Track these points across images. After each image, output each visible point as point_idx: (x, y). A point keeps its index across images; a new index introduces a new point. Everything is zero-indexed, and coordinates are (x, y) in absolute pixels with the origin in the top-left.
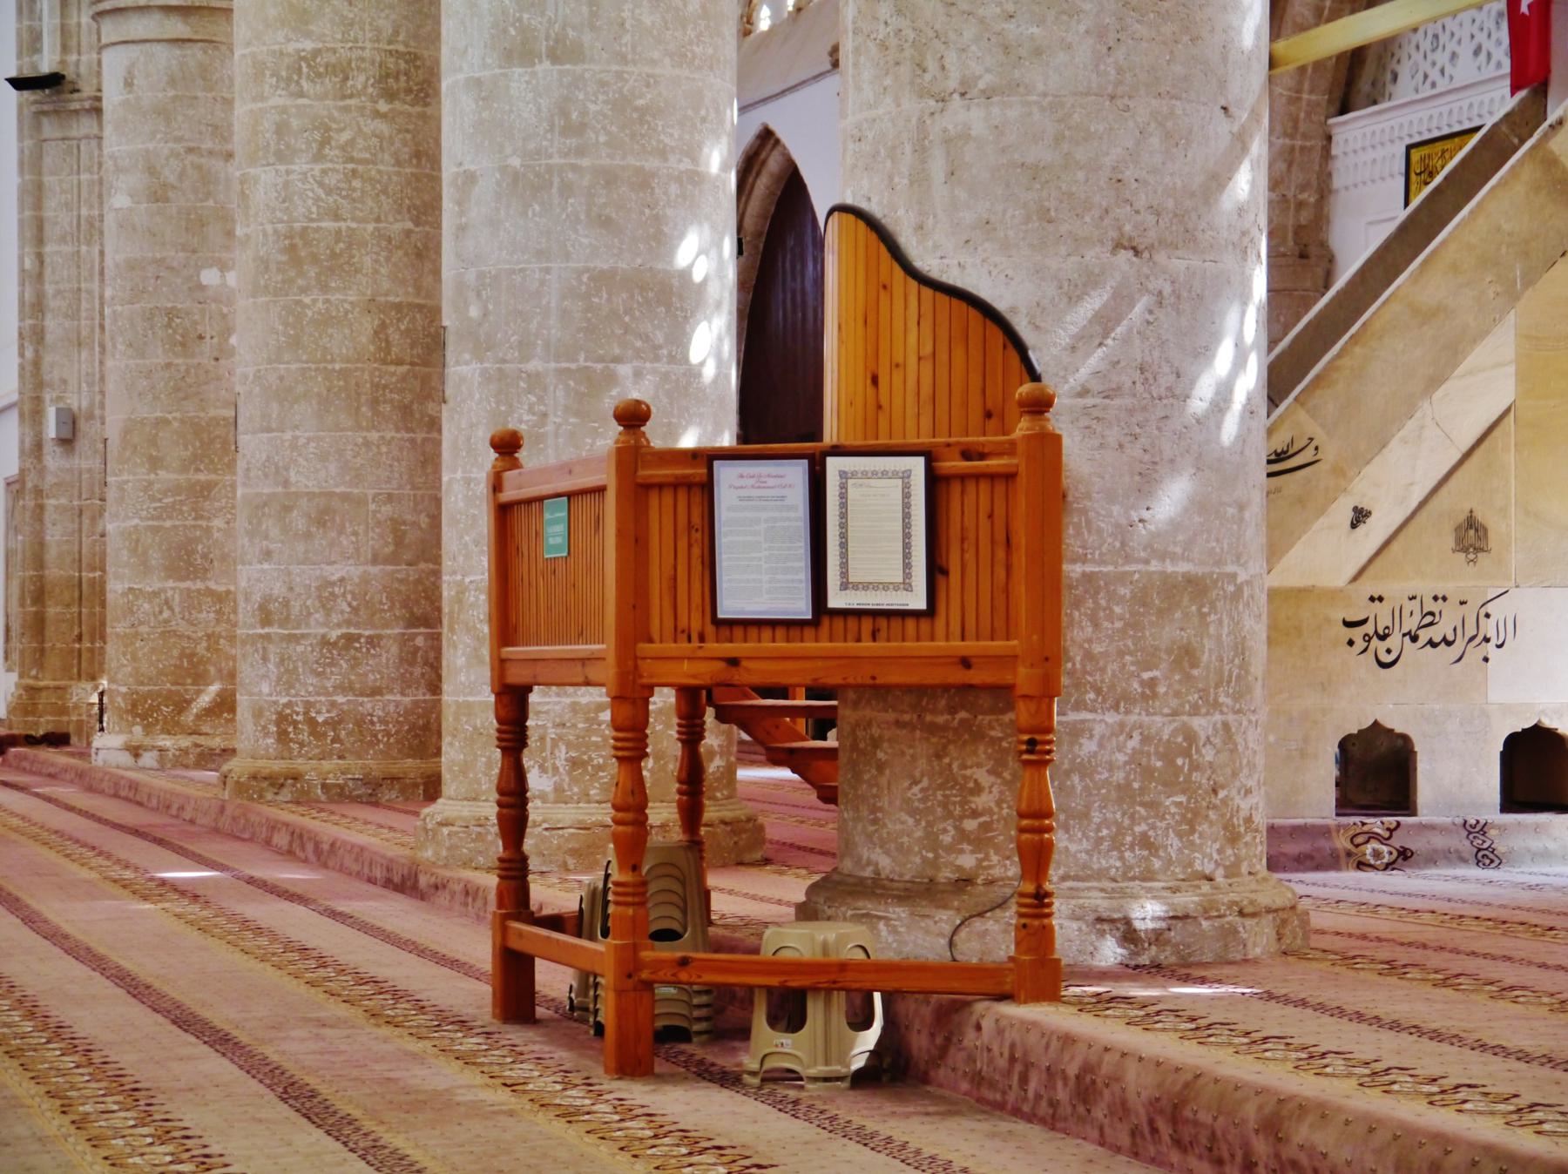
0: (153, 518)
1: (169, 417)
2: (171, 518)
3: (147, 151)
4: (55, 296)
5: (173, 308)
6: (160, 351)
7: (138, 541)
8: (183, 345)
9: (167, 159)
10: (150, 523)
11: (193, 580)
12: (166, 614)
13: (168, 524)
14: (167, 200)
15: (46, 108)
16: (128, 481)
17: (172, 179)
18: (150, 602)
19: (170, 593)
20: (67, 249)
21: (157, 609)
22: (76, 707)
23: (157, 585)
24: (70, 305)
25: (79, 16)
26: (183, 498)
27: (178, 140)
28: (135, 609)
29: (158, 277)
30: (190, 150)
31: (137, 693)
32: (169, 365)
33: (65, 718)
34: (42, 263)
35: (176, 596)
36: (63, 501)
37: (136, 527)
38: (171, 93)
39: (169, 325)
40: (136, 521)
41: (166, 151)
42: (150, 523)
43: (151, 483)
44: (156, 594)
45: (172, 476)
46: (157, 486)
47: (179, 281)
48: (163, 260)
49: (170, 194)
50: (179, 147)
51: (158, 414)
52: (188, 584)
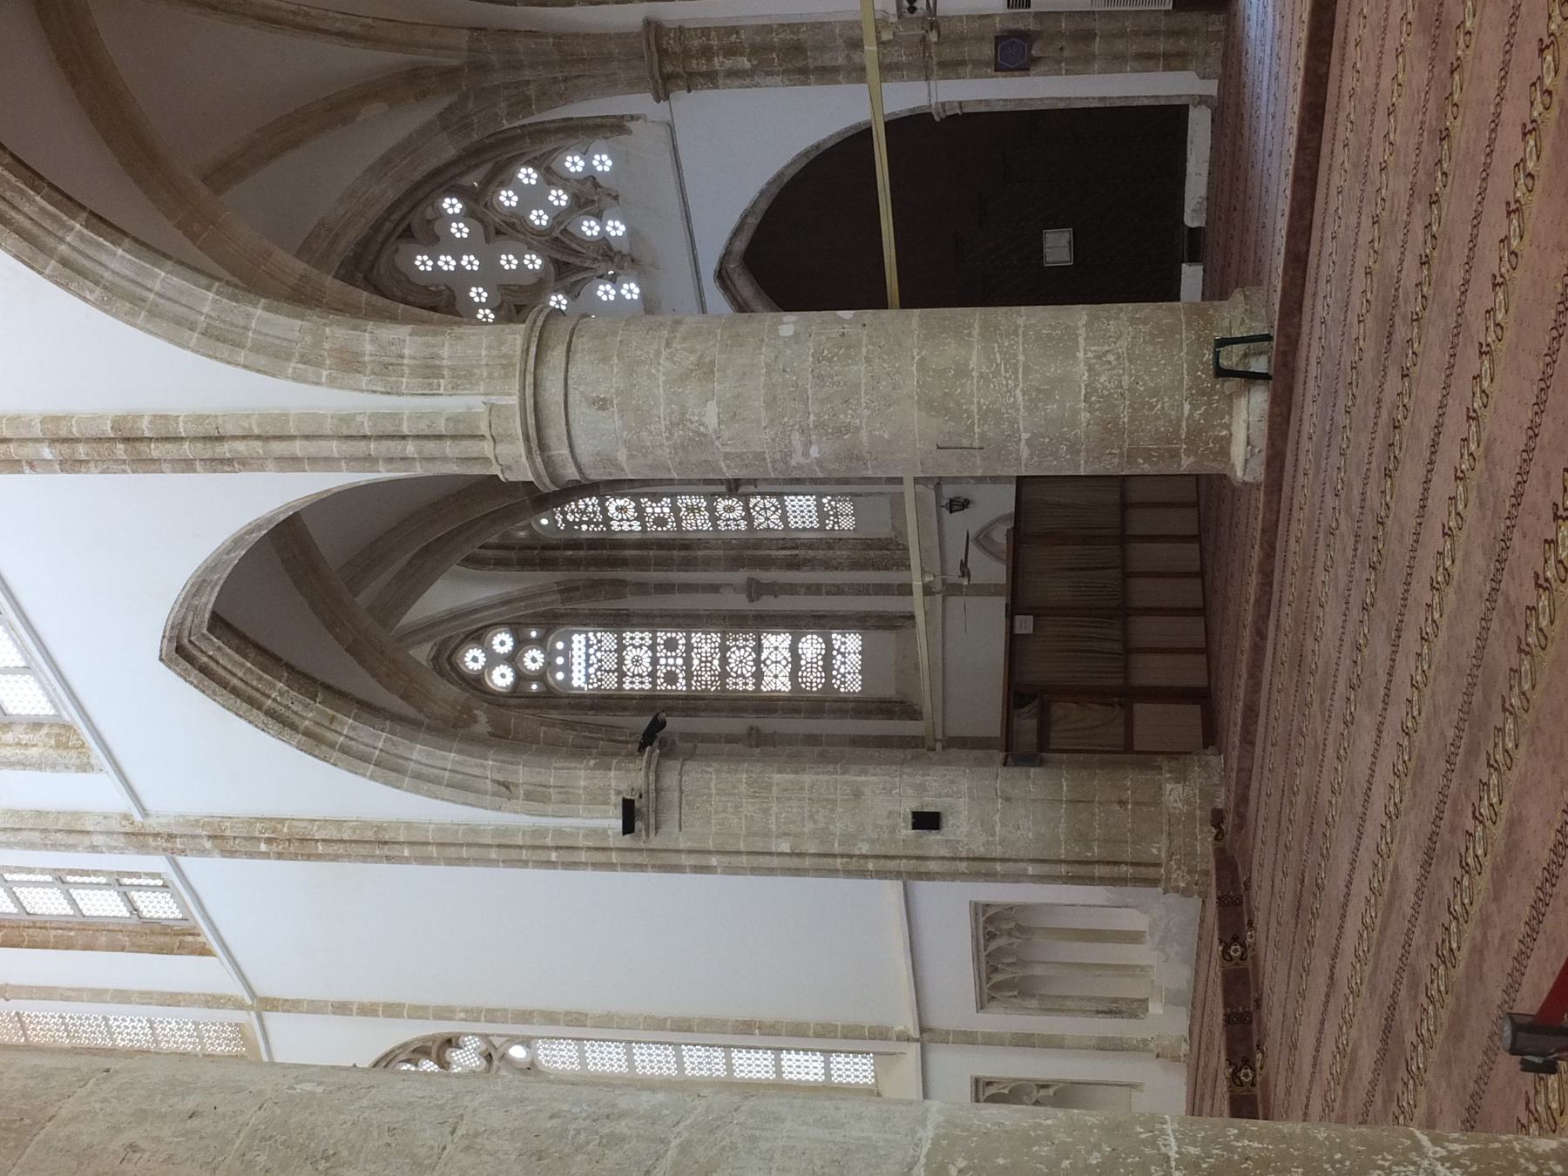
0: (1016, 373)
1: (917, 358)
2: (1015, 356)
3: (665, 382)
4: (815, 822)
5: (813, 355)
6: (855, 368)
7: (1039, 390)
8: (849, 347)
9: (674, 363)
10: (1020, 376)
11: (1077, 336)
12: (1111, 358)
13: (1021, 358)
14: (712, 362)
15: (652, 821)
16: (979, 403)
17: (693, 358)
18: (1099, 374)
19: (1090, 355)
20: (774, 808)
21: (1106, 367)
22: (1187, 802)
23: (1082, 367)
24: (823, 807)
25: (579, 788)
26: (996, 345)
27: (658, 354)
28: (1106, 393)
29: (784, 371)
30: (668, 345)
31: (1190, 388)
32: (868, 360)
33: (1198, 812)
34: (785, 834)
35: (1092, 349)
36: (997, 818)
37: (1024, 393)
38: (615, 360)
39: (830, 361)
40: (1018, 392)
41: (668, 364)
42: (1020, 376)
43: (981, 376)
44: (1091, 369)
45: (974, 358)
46: (984, 369)
47: (788, 352)
48: (767, 366)
49: (707, 360)
50: (664, 354)
51: (914, 368)
52: (1081, 340)
